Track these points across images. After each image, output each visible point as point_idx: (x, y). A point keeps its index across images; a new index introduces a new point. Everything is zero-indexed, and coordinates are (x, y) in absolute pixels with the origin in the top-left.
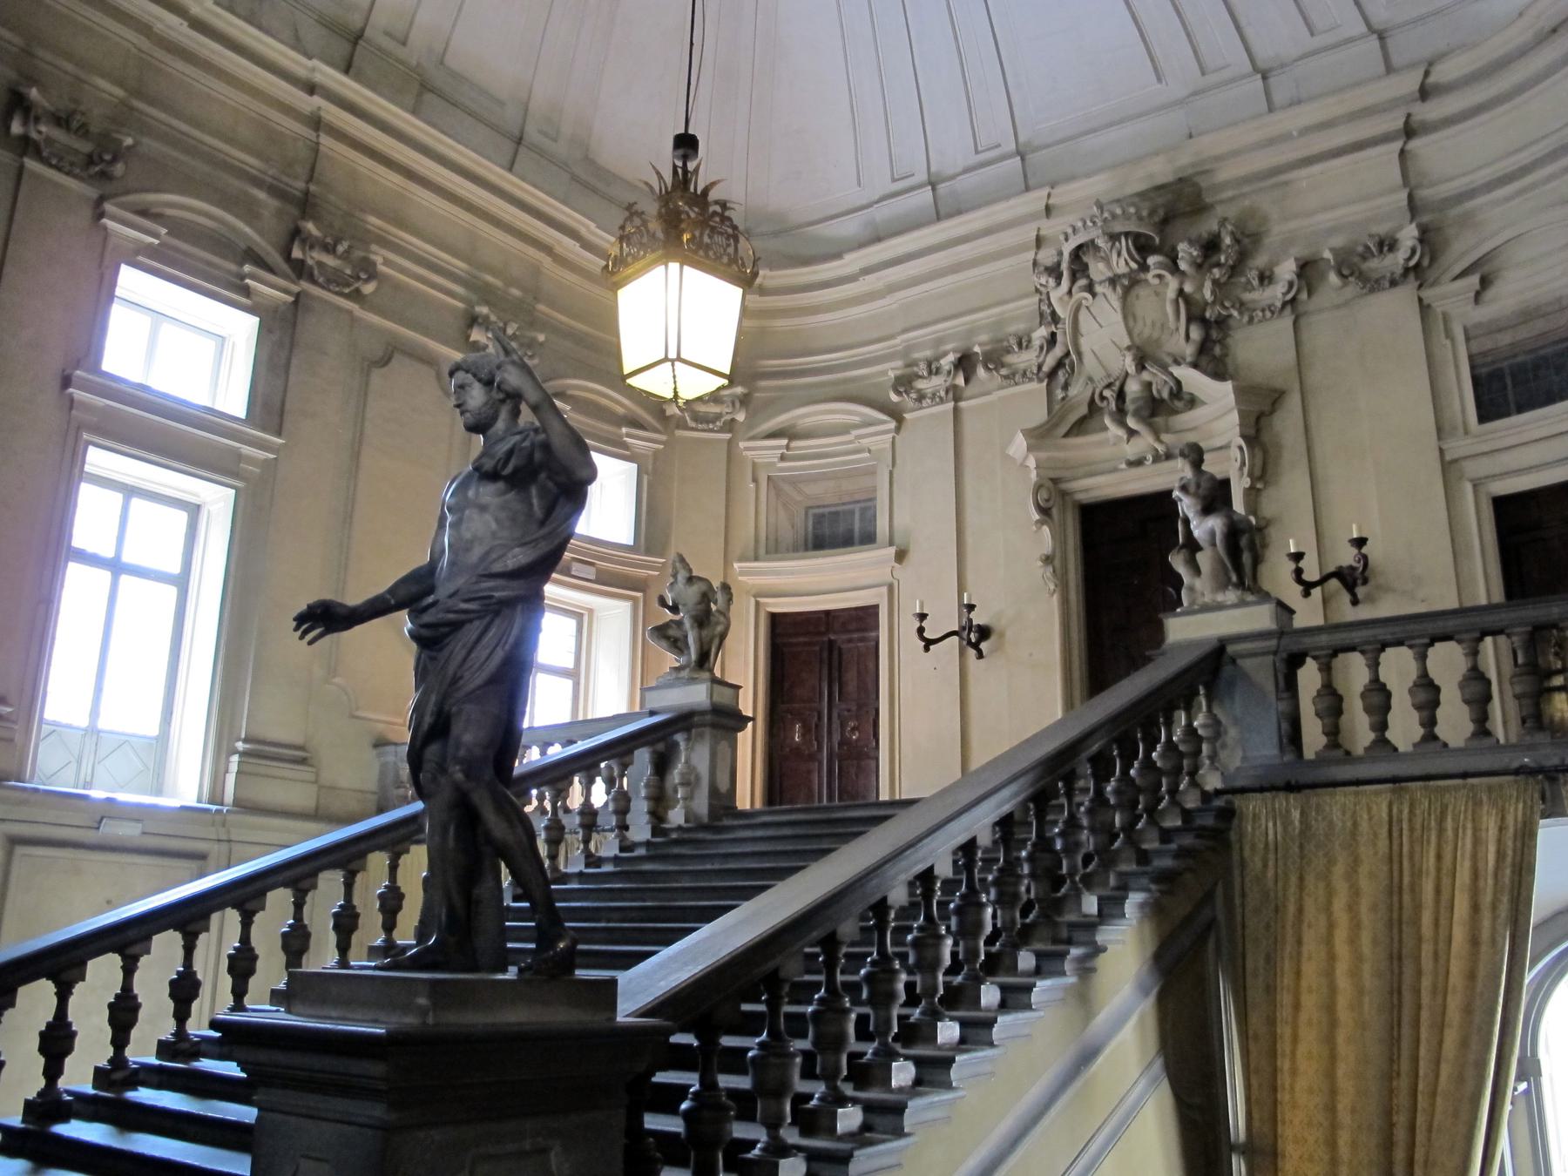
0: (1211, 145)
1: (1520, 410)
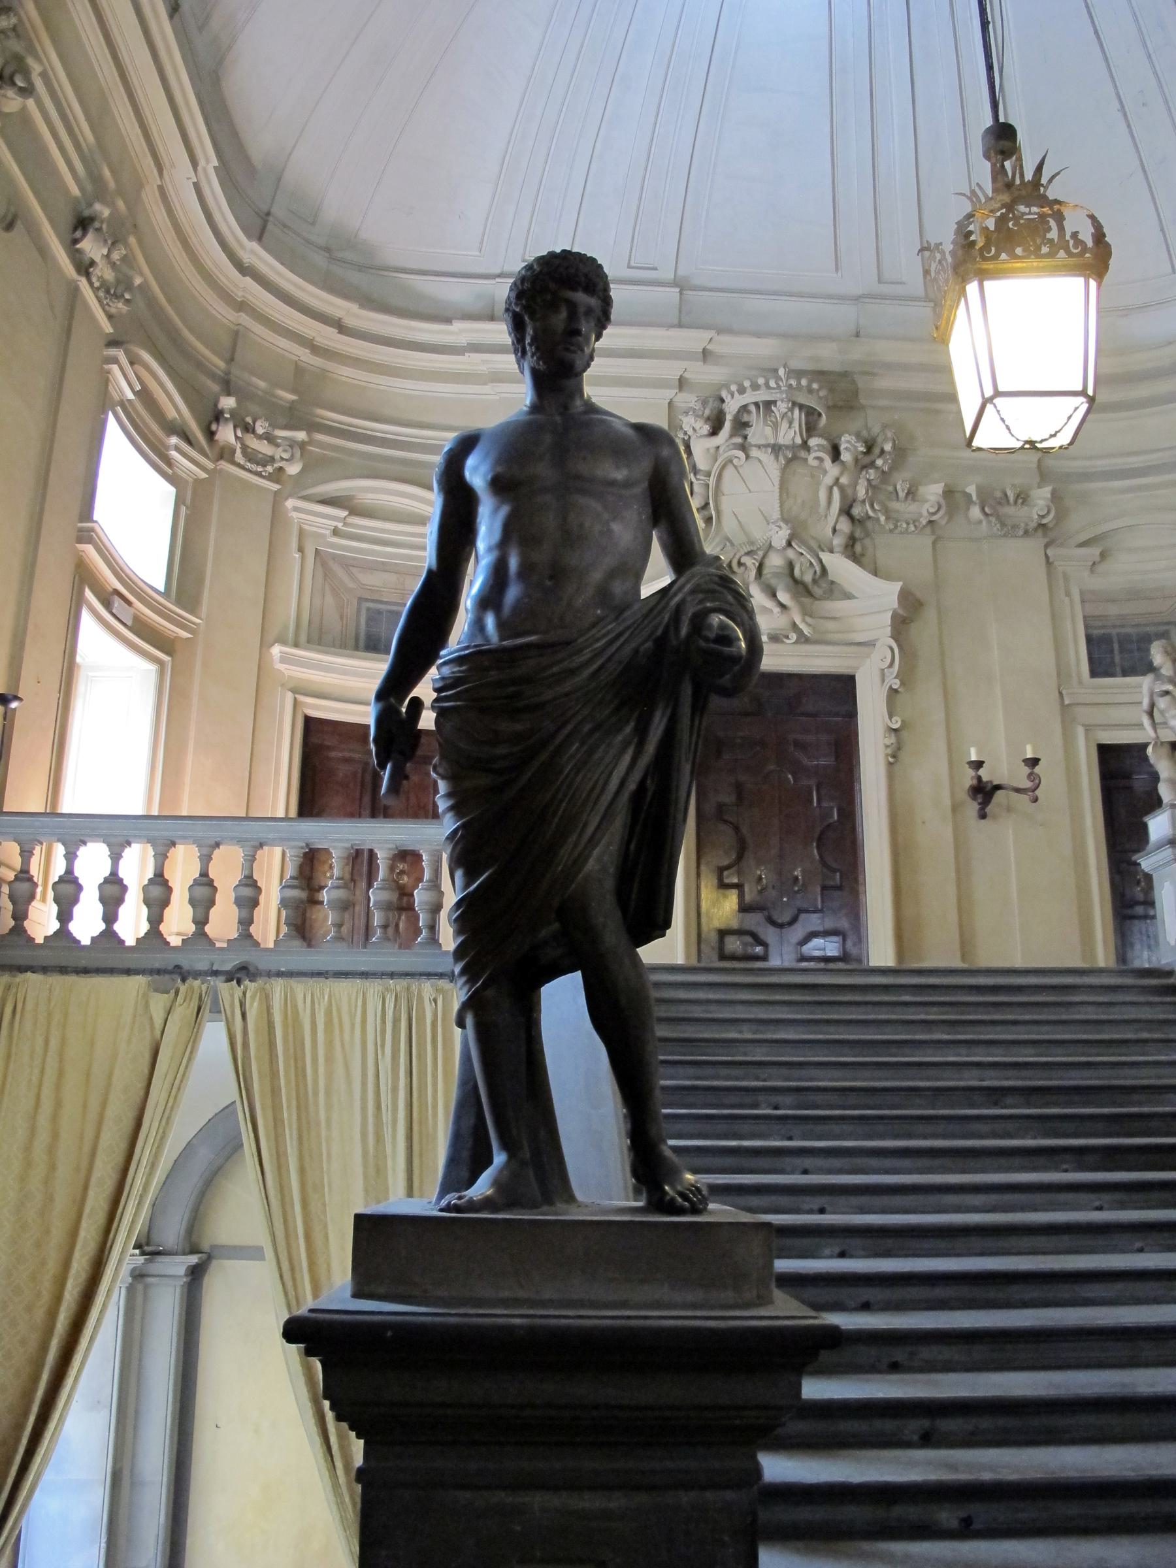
0: (887, 351)
1: (1125, 673)
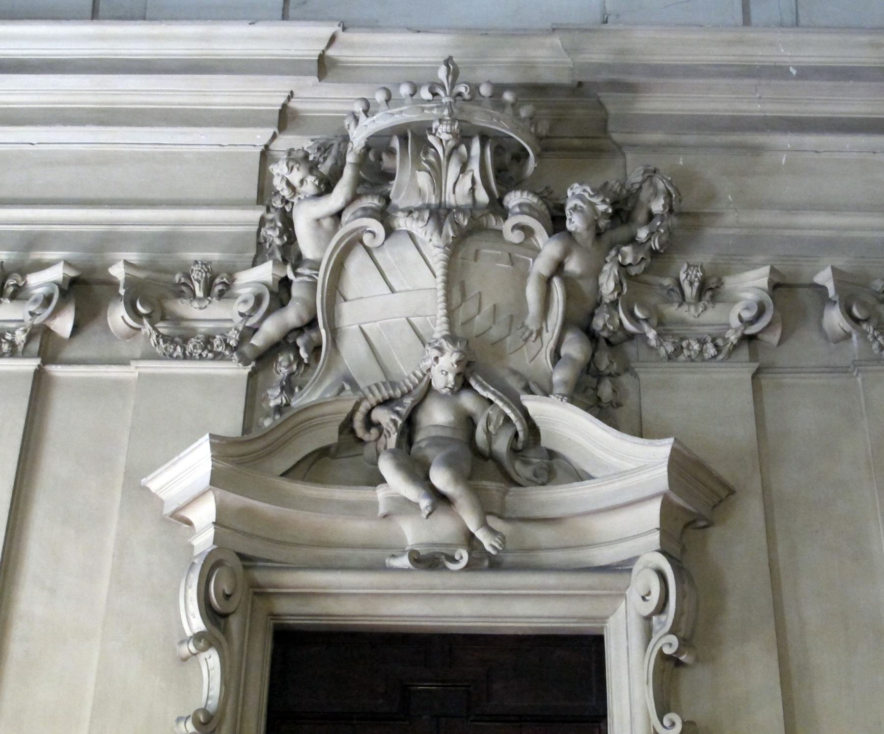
0: (651, 44)
